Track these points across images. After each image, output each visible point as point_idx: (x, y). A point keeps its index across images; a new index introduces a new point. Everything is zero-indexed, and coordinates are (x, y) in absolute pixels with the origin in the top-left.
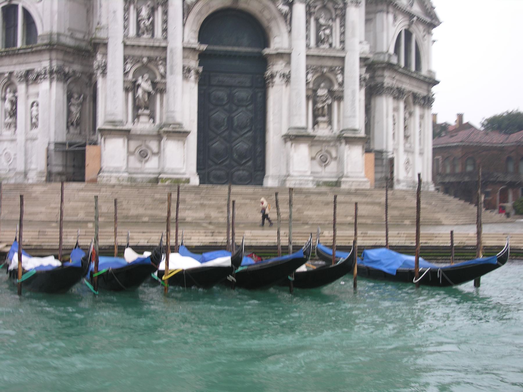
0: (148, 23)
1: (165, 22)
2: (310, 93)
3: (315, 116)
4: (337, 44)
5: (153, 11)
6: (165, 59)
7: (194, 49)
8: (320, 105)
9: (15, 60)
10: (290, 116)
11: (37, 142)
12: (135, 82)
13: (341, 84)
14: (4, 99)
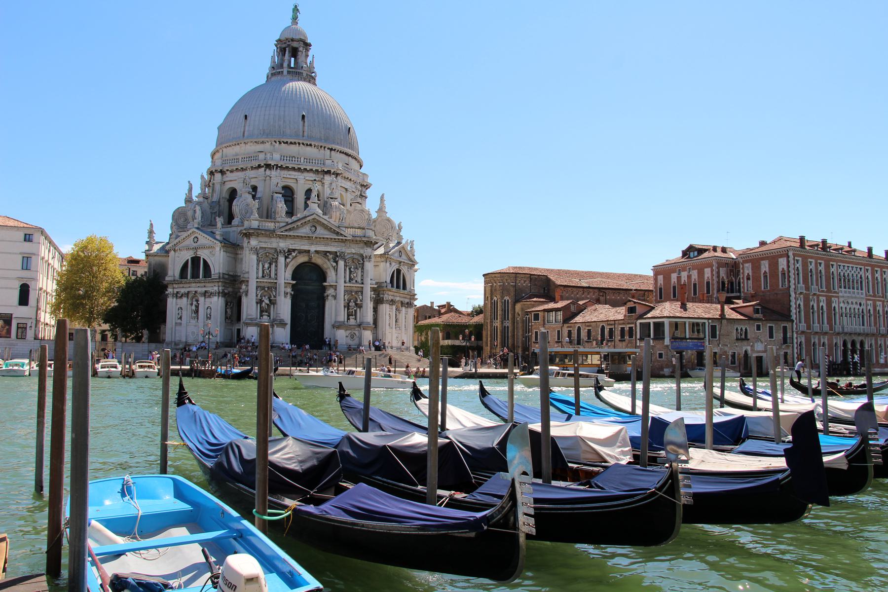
0: (268, 271)
1: (276, 270)
2: (346, 305)
3: (348, 316)
4: (359, 280)
5: (270, 264)
6: (276, 288)
7: (290, 283)
8: (350, 311)
9: (198, 285)
10: (336, 315)
12: (261, 300)
14: (192, 304)
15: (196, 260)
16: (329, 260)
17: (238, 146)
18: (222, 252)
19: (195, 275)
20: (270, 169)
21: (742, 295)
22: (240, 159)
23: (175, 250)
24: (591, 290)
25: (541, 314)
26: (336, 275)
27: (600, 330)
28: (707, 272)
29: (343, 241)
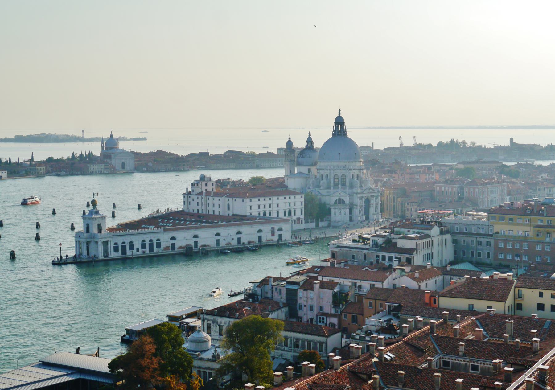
15: (340, 199)
23: (333, 196)
25: (409, 204)
28: (454, 189)
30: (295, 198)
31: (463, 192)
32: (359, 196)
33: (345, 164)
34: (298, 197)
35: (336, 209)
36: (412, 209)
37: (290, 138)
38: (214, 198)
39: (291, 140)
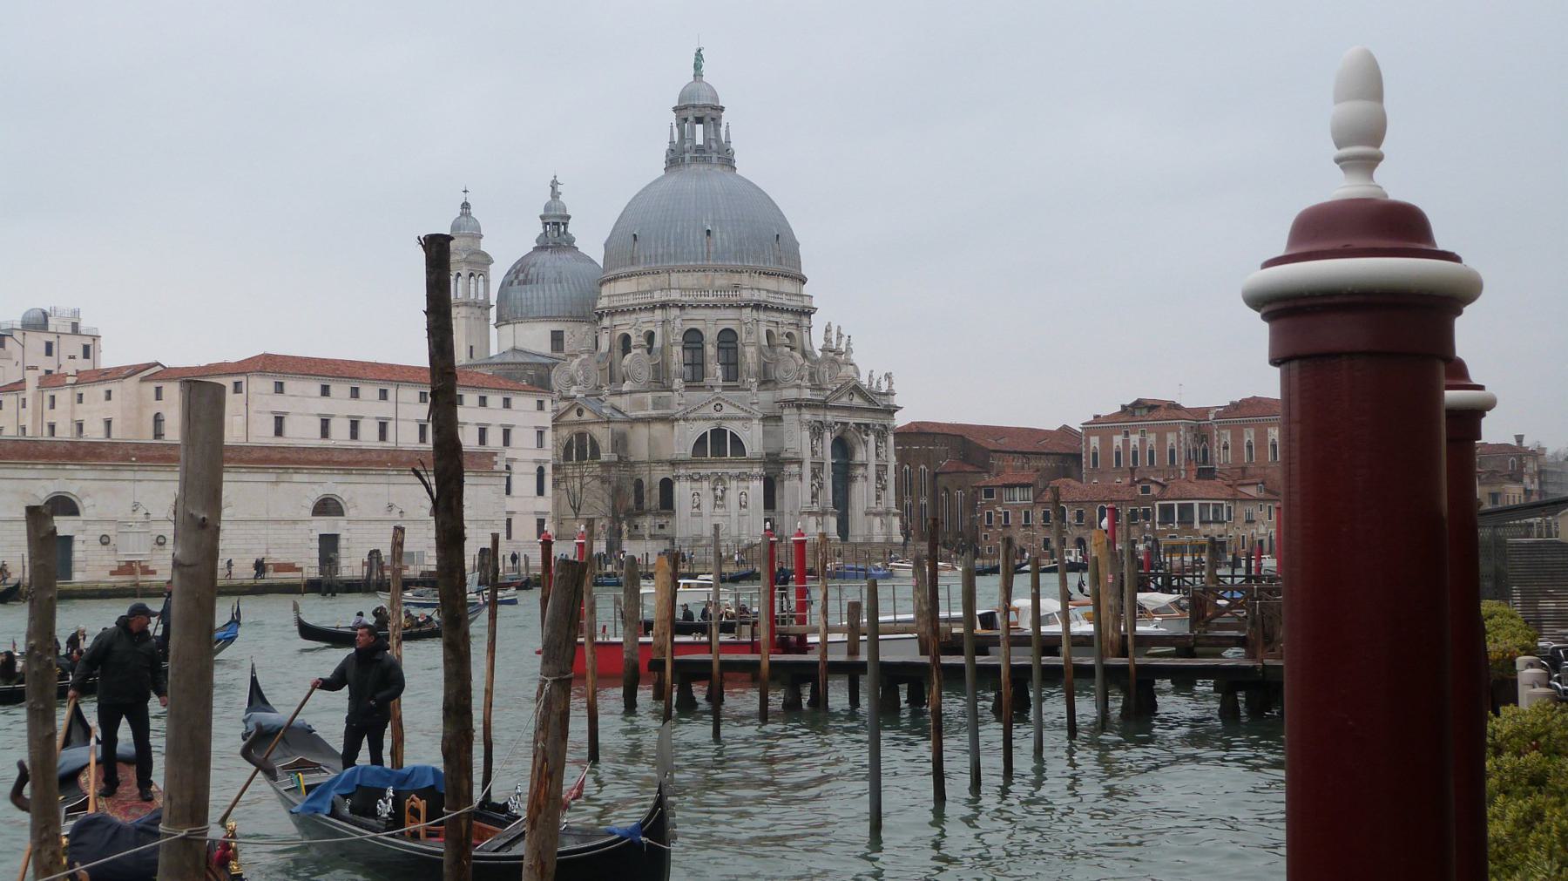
5: (818, 440)
9: (726, 465)
11: (747, 517)
13: (885, 481)
14: (715, 489)
15: (719, 434)
16: (860, 433)
17: (700, 273)
18: (761, 426)
19: (719, 450)
20: (758, 310)
21: (1217, 467)
22: (711, 292)
23: (686, 420)
24: (1015, 455)
26: (866, 451)
27: (1097, 511)
28: (1171, 438)
29: (875, 411)
30: (507, 403)
31: (1205, 451)
32: (807, 415)
33: (736, 279)
34: (524, 403)
35: (701, 479)
36: (1006, 514)
37: (466, 206)
38: (80, 390)
39: (474, 212)
